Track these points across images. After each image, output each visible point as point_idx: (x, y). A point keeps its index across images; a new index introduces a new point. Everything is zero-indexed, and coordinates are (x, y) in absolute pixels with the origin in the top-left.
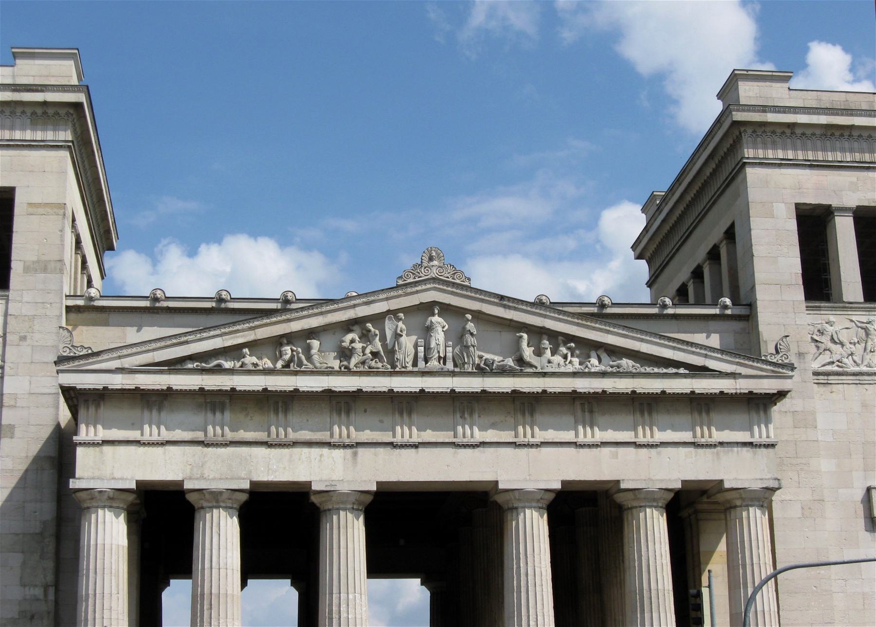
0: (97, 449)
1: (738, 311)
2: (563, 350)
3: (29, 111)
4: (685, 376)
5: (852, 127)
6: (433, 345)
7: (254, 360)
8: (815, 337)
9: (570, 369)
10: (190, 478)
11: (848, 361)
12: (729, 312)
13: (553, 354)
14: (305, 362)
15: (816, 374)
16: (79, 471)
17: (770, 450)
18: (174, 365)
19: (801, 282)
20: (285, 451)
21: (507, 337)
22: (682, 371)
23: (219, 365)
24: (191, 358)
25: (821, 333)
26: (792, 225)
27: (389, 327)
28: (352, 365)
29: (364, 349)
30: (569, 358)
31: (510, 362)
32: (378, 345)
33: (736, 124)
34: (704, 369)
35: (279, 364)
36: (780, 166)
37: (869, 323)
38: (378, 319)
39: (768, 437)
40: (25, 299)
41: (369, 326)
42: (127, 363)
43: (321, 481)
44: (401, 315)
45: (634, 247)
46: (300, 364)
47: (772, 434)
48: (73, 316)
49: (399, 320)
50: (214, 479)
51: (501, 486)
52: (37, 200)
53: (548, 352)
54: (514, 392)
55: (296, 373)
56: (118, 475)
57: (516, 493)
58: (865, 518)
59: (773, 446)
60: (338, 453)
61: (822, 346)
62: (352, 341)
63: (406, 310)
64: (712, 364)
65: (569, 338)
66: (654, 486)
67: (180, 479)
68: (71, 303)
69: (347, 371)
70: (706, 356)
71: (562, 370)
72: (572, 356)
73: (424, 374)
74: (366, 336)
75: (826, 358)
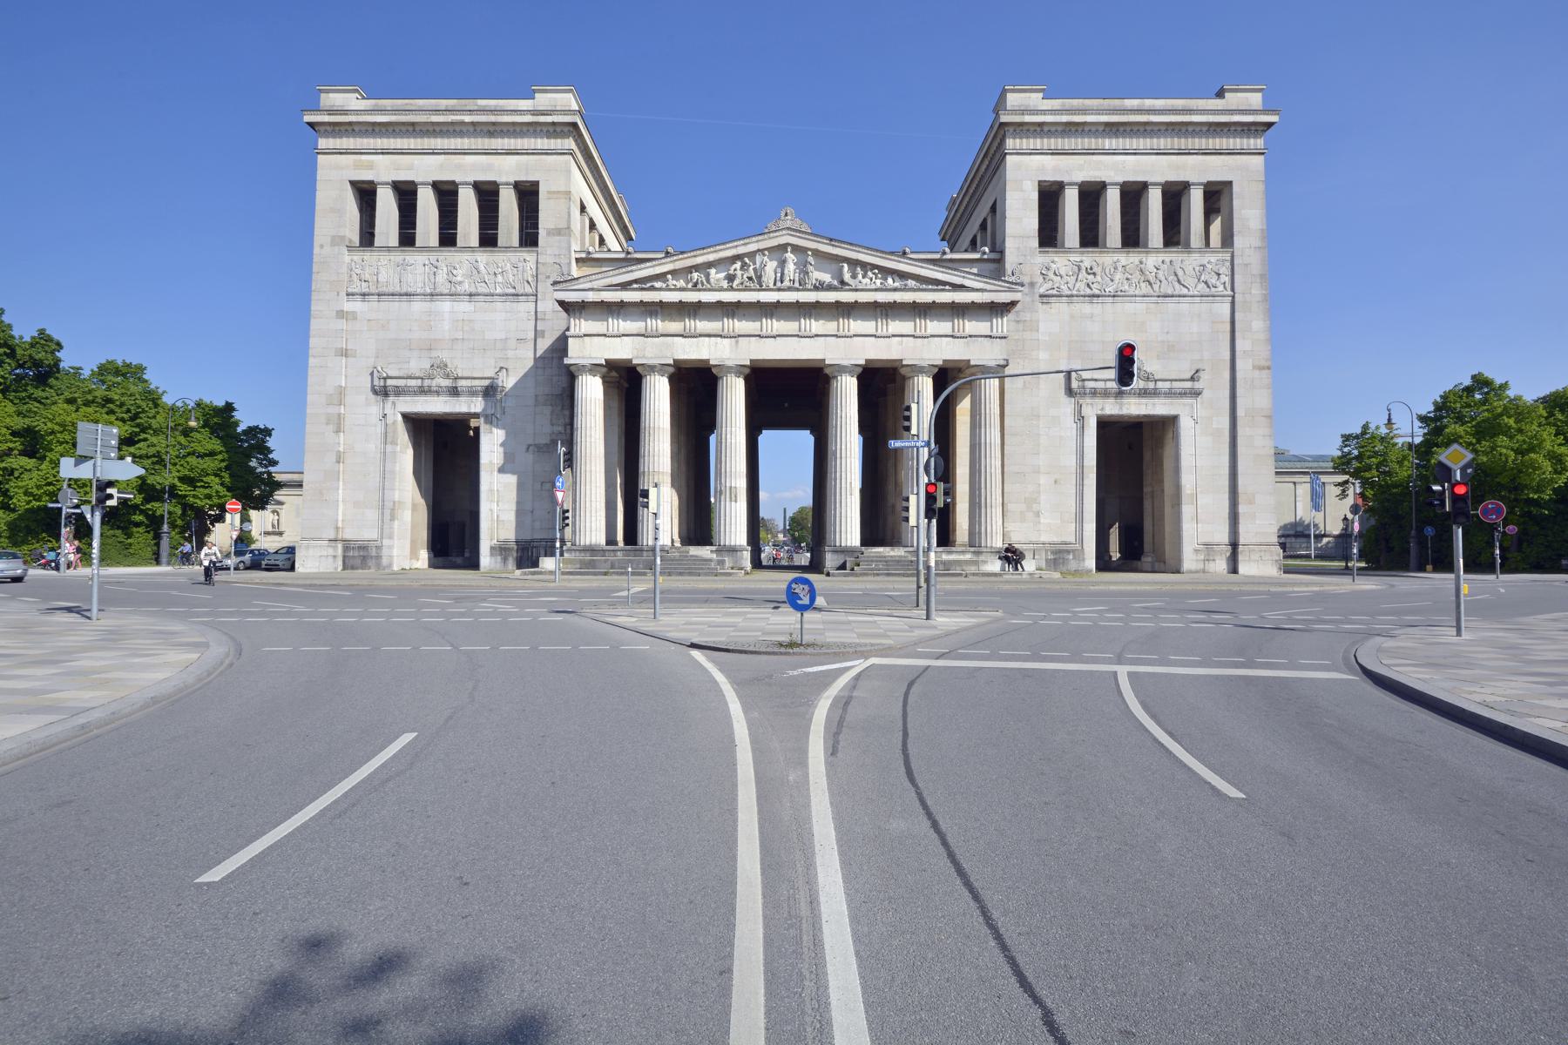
0: (581, 339)
1: (993, 256)
2: (870, 274)
3: (545, 129)
4: (949, 291)
5: (1085, 123)
6: (786, 272)
7: (674, 282)
8: (1043, 272)
9: (873, 287)
10: (637, 357)
11: (1064, 287)
12: (986, 257)
13: (863, 277)
14: (705, 283)
15: (1041, 296)
16: (570, 354)
17: (1003, 340)
18: (624, 286)
19: (1037, 235)
20: (695, 339)
21: (834, 266)
22: (947, 287)
23: (652, 286)
24: (636, 281)
26: (1035, 196)
27: (758, 258)
28: (734, 286)
29: (742, 275)
30: (874, 280)
31: (835, 283)
32: (751, 273)
33: (1003, 125)
36: (1030, 154)
37: (1082, 262)
38: (752, 255)
39: (1002, 332)
40: (548, 253)
41: (746, 260)
42: (596, 284)
43: (716, 359)
44: (766, 253)
46: (703, 284)
47: (1005, 330)
48: (580, 264)
49: (764, 255)
50: (651, 358)
51: (827, 363)
52: (554, 189)
53: (860, 276)
54: (837, 302)
55: (699, 290)
56: (593, 355)
57: (837, 368)
58: (1066, 389)
59: (1005, 338)
60: (726, 341)
61: (1048, 278)
62: (735, 270)
63: (769, 249)
64: (967, 283)
65: (874, 267)
66: (925, 364)
67: (630, 357)
68: (578, 256)
69: (731, 289)
70: (964, 277)
71: (868, 287)
72: (876, 279)
73: (779, 290)
75: (1049, 285)
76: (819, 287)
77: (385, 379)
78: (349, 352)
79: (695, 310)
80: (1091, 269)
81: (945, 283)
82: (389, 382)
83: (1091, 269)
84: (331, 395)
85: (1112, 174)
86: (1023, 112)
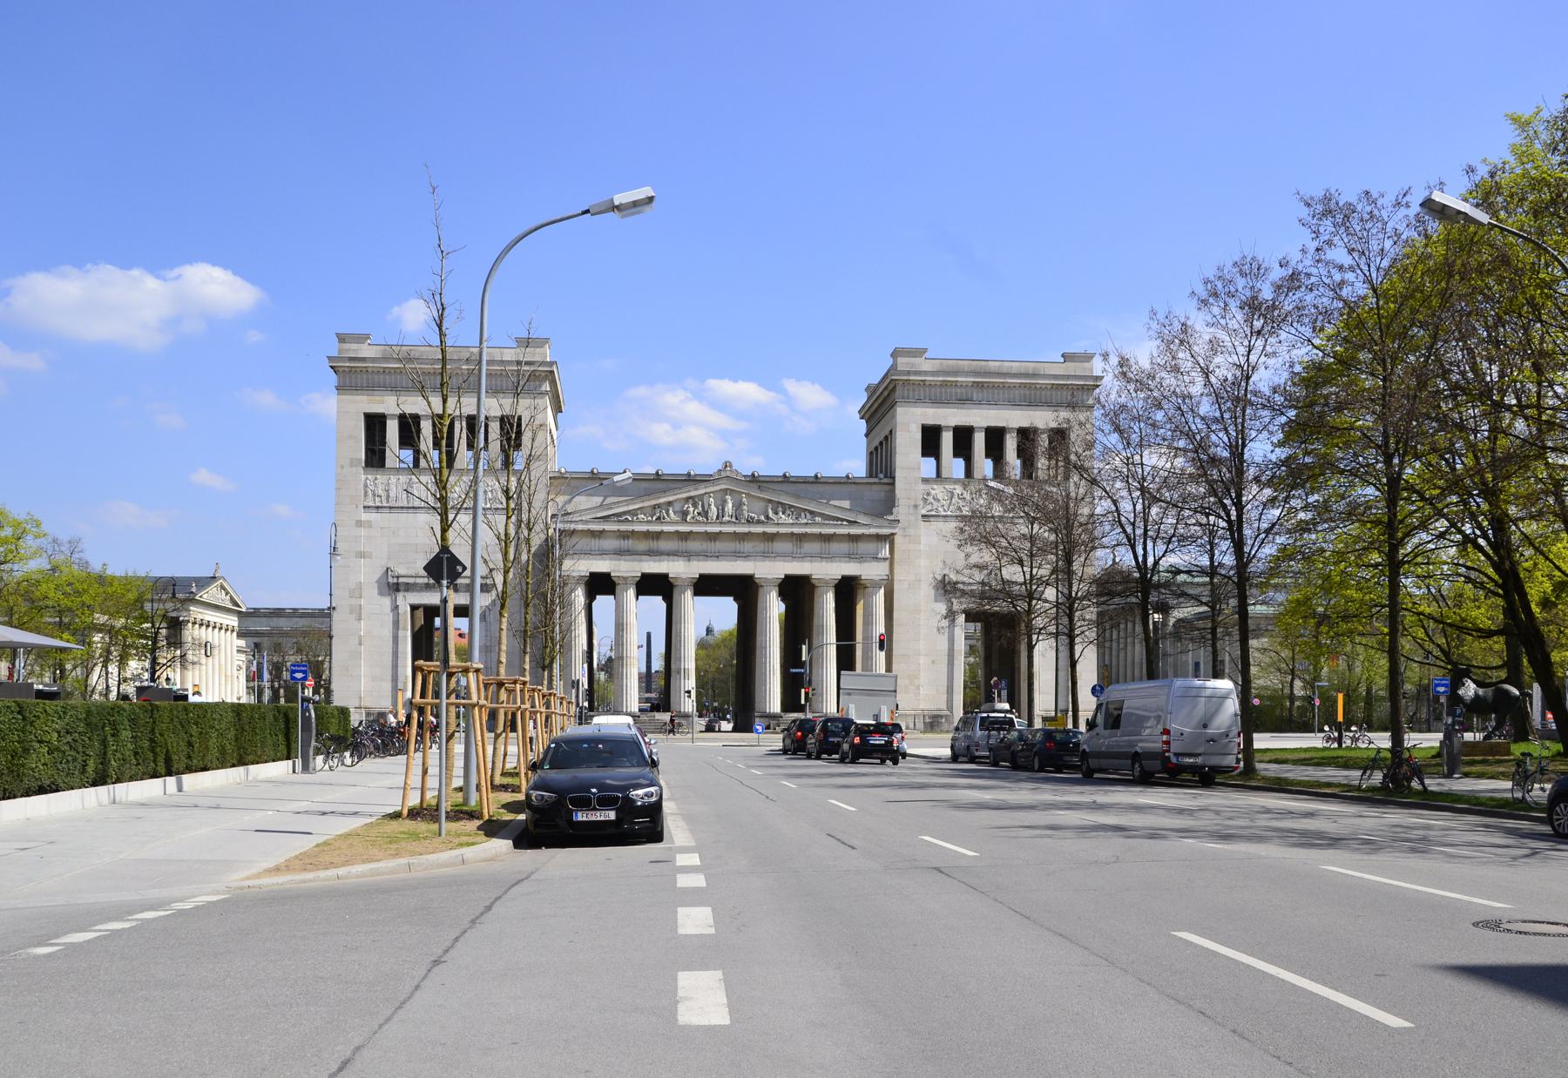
1: (886, 481)
7: (643, 516)
15: (923, 516)
18: (605, 518)
22: (845, 523)
25: (928, 494)
31: (762, 518)
34: (856, 522)
35: (654, 518)
38: (701, 497)
41: (696, 500)
45: (860, 412)
65: (791, 507)
67: (609, 571)
74: (695, 506)
75: (929, 507)
76: (750, 521)
77: (398, 577)
78: (366, 554)
79: (657, 536)
80: (962, 495)
81: (843, 520)
82: (401, 580)
83: (962, 495)
84: (353, 590)
85: (979, 419)
86: (909, 373)
